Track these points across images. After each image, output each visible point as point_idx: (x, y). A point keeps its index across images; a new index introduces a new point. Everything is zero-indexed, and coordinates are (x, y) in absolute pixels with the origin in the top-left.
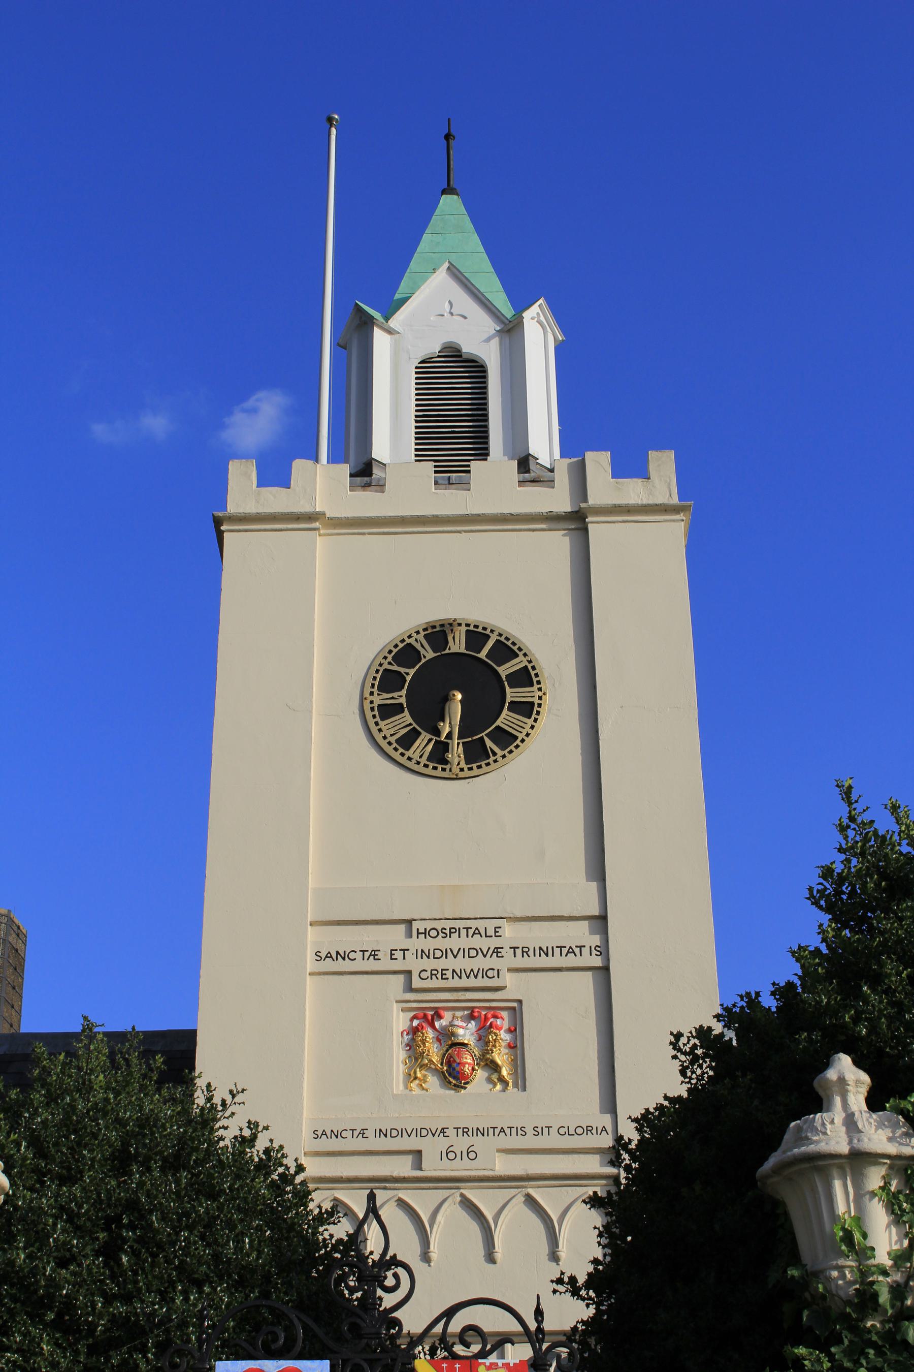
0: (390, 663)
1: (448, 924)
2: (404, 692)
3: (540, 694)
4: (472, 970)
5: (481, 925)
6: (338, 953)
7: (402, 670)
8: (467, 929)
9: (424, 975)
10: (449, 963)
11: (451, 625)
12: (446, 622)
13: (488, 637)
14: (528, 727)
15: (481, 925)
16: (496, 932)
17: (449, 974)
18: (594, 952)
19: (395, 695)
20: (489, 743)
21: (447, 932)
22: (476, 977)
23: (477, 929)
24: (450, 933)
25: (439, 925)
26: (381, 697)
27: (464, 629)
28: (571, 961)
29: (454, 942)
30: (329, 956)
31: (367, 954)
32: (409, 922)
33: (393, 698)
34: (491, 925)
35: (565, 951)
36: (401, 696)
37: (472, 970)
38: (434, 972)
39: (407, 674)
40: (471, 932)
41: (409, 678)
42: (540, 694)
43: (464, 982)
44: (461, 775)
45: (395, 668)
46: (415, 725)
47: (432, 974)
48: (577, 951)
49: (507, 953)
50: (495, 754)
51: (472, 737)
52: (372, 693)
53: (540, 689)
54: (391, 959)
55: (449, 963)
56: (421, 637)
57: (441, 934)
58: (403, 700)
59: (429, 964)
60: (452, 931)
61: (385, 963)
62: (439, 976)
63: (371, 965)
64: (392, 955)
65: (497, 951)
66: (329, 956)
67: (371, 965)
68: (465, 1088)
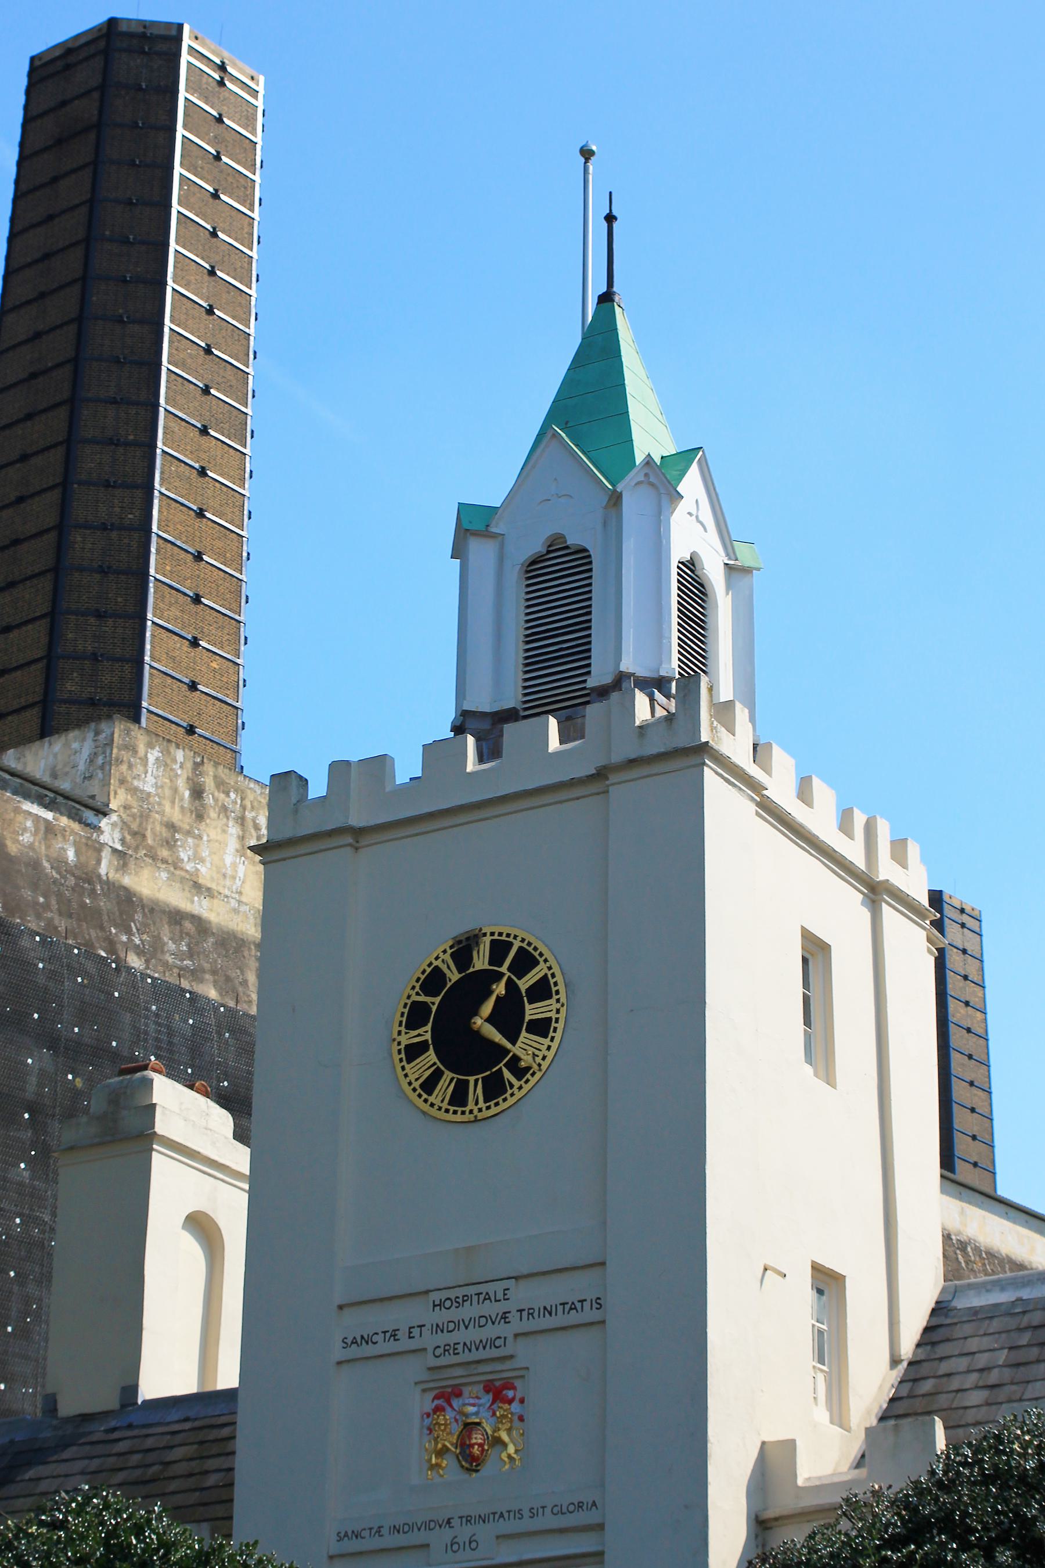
0: (417, 994)
1: (460, 1292)
2: (429, 1027)
3: (558, 1006)
4: (481, 1341)
5: (490, 1288)
6: (362, 1337)
7: (428, 999)
8: (478, 1294)
9: (438, 1352)
10: (461, 1336)
11: (476, 936)
12: (471, 934)
13: (511, 944)
14: (544, 1048)
15: (490, 1288)
16: (505, 1294)
17: (460, 1347)
18: (595, 1305)
19: (420, 1031)
20: (507, 1074)
21: (460, 1300)
22: (484, 1348)
23: (487, 1293)
24: (464, 1301)
25: (452, 1294)
26: (408, 1036)
27: (488, 939)
28: (574, 1318)
29: (467, 1312)
30: (354, 1342)
31: (388, 1335)
32: (427, 1292)
33: (419, 1035)
34: (499, 1287)
35: (567, 1307)
36: (425, 1033)
37: (481, 1341)
38: (447, 1348)
39: (433, 1004)
40: (482, 1297)
41: (434, 1008)
42: (558, 1006)
43: (475, 1355)
44: (480, 1116)
45: (422, 998)
46: (439, 1064)
47: (445, 1350)
48: (578, 1305)
49: (514, 1317)
50: (512, 1086)
51: (490, 1069)
52: (399, 1033)
53: (558, 1001)
54: (410, 1337)
55: (461, 1336)
56: (447, 957)
57: (455, 1304)
58: (428, 1036)
59: (442, 1339)
60: (466, 1298)
61: (404, 1344)
62: (451, 1351)
63: (391, 1346)
64: (410, 1333)
65: (505, 1316)
66: (354, 1342)
67: (391, 1346)
68: (477, 1471)
